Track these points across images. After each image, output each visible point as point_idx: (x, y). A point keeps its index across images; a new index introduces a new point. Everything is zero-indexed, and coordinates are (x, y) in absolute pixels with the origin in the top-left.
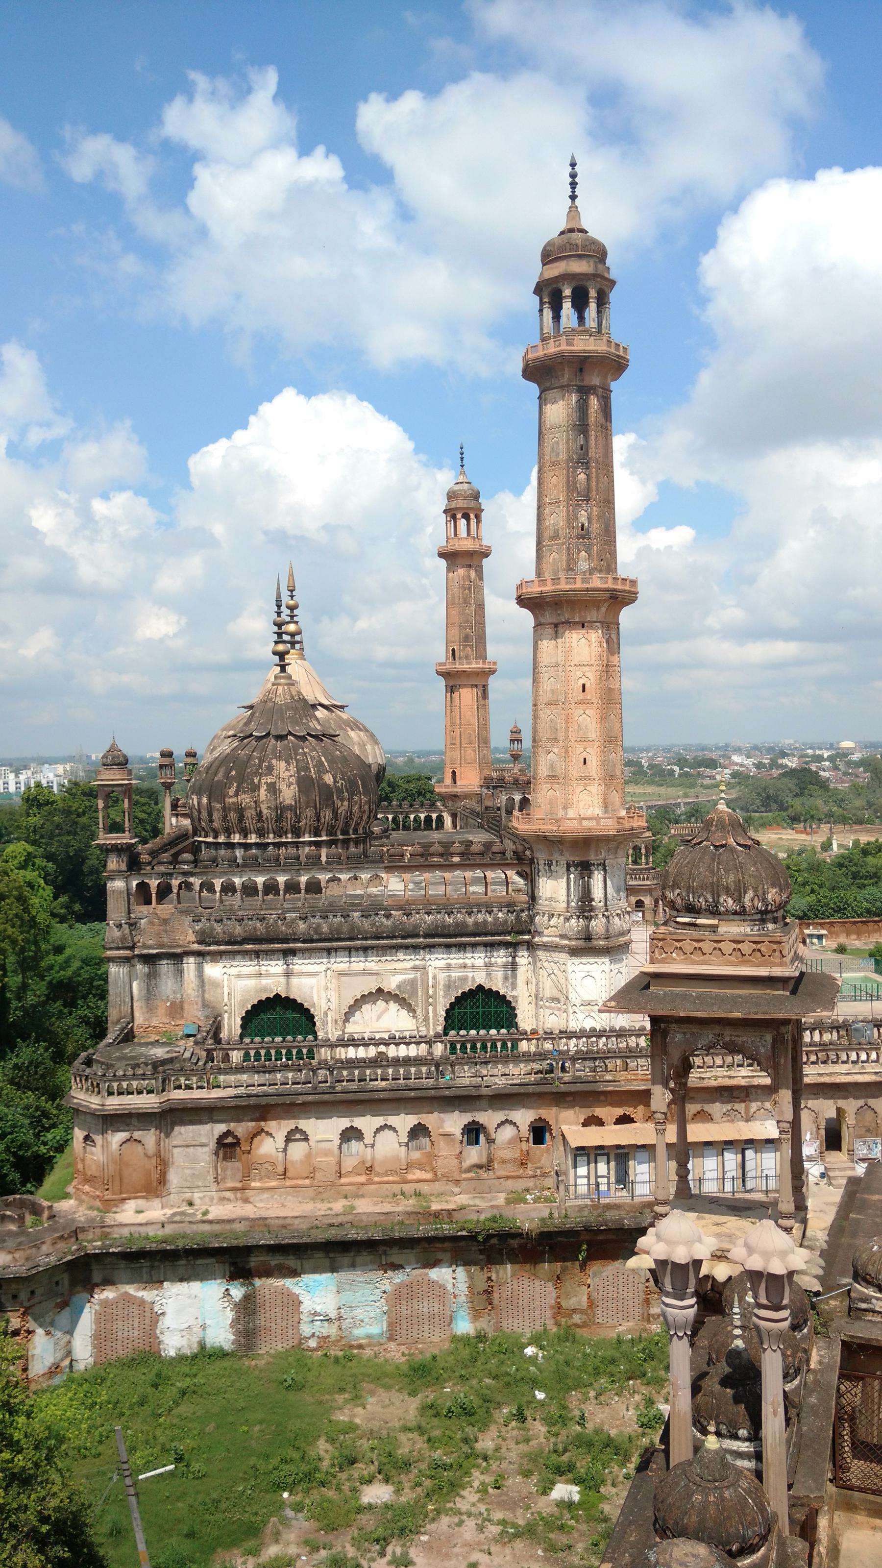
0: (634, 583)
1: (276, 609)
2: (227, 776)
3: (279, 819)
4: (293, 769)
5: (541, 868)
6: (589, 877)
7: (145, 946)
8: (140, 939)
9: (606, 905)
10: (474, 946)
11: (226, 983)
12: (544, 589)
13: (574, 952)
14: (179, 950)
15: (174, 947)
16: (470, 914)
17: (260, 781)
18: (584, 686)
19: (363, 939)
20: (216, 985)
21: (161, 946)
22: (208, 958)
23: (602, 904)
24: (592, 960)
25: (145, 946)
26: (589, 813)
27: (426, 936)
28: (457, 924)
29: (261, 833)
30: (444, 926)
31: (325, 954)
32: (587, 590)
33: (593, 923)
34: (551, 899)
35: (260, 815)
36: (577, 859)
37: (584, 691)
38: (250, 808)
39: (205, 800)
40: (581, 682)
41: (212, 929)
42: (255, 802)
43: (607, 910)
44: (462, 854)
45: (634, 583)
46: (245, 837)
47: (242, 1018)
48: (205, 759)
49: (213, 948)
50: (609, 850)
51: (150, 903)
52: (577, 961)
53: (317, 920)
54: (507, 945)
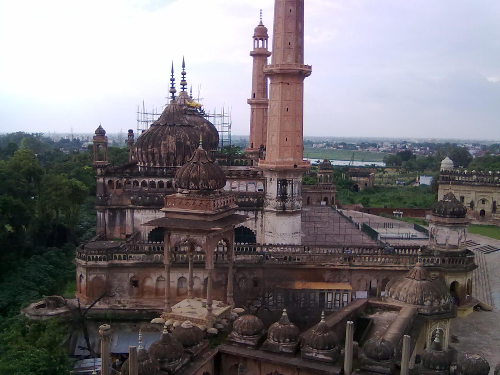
0: (310, 67)
1: (171, 74)
2: (148, 140)
3: (168, 158)
5: (268, 181)
7: (111, 205)
8: (109, 202)
11: (142, 220)
12: (273, 68)
13: (278, 214)
15: (122, 206)
16: (240, 198)
17: (161, 143)
18: (287, 109)
20: (138, 221)
21: (118, 205)
22: (136, 211)
23: (291, 196)
24: (285, 218)
25: (111, 205)
26: (287, 160)
29: (161, 164)
32: (290, 69)
33: (287, 204)
34: (271, 193)
35: (161, 156)
36: (281, 178)
37: (287, 111)
38: (157, 153)
39: (140, 150)
40: (287, 107)
41: (137, 198)
42: (159, 151)
43: (292, 199)
44: (236, 175)
45: (310, 67)
46: (155, 165)
47: (149, 234)
48: (138, 133)
49: (138, 206)
50: (294, 175)
51: (114, 189)
52: (279, 218)
54: (253, 210)
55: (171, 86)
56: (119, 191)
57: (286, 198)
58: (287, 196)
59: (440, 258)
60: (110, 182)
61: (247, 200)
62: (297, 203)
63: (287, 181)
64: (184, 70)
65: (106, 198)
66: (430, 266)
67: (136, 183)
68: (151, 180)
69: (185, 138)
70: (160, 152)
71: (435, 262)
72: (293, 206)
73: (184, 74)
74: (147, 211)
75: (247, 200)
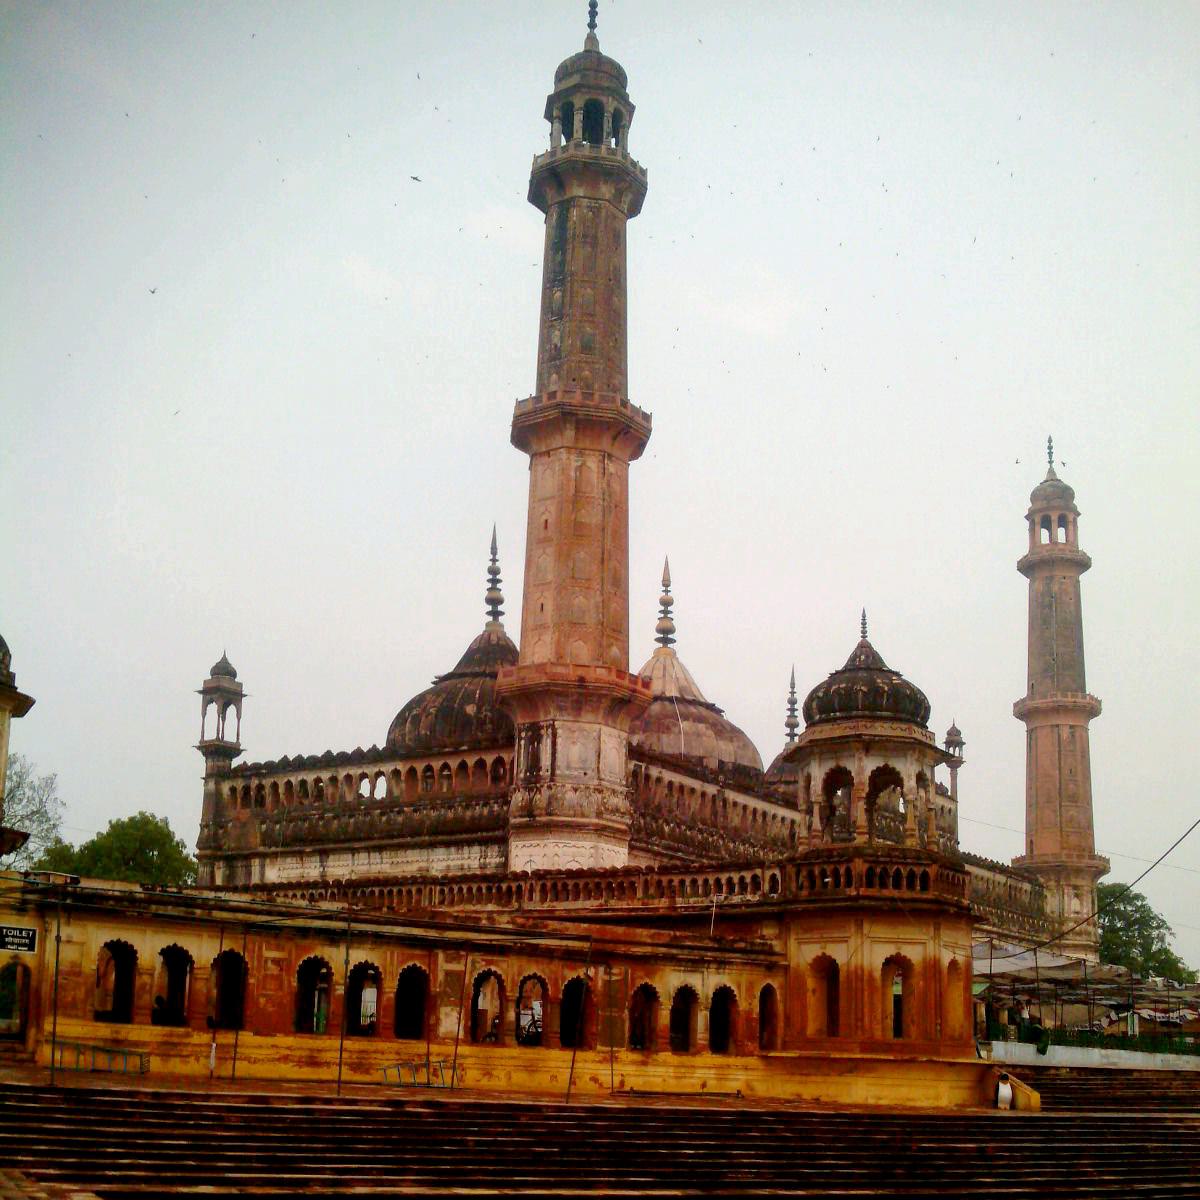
4: (440, 700)
6: (538, 744)
9: (553, 774)
10: (470, 843)
14: (246, 852)
16: (467, 807)
19: (379, 838)
22: (268, 861)
24: (534, 842)
27: (430, 834)
28: (458, 820)
30: (445, 822)
31: (350, 856)
43: (552, 780)
49: (273, 849)
50: (560, 709)
53: (344, 820)
55: (490, 585)
56: (246, 814)
57: (538, 779)
58: (541, 773)
59: (777, 872)
60: (233, 790)
61: (486, 811)
62: (570, 796)
63: (542, 727)
64: (667, 591)
65: (221, 831)
66: (748, 904)
67: (275, 786)
68: (300, 778)
69: (469, 698)
70: (403, 736)
71: (766, 887)
72: (555, 804)
73: (666, 603)
74: (289, 860)
75: (486, 811)
